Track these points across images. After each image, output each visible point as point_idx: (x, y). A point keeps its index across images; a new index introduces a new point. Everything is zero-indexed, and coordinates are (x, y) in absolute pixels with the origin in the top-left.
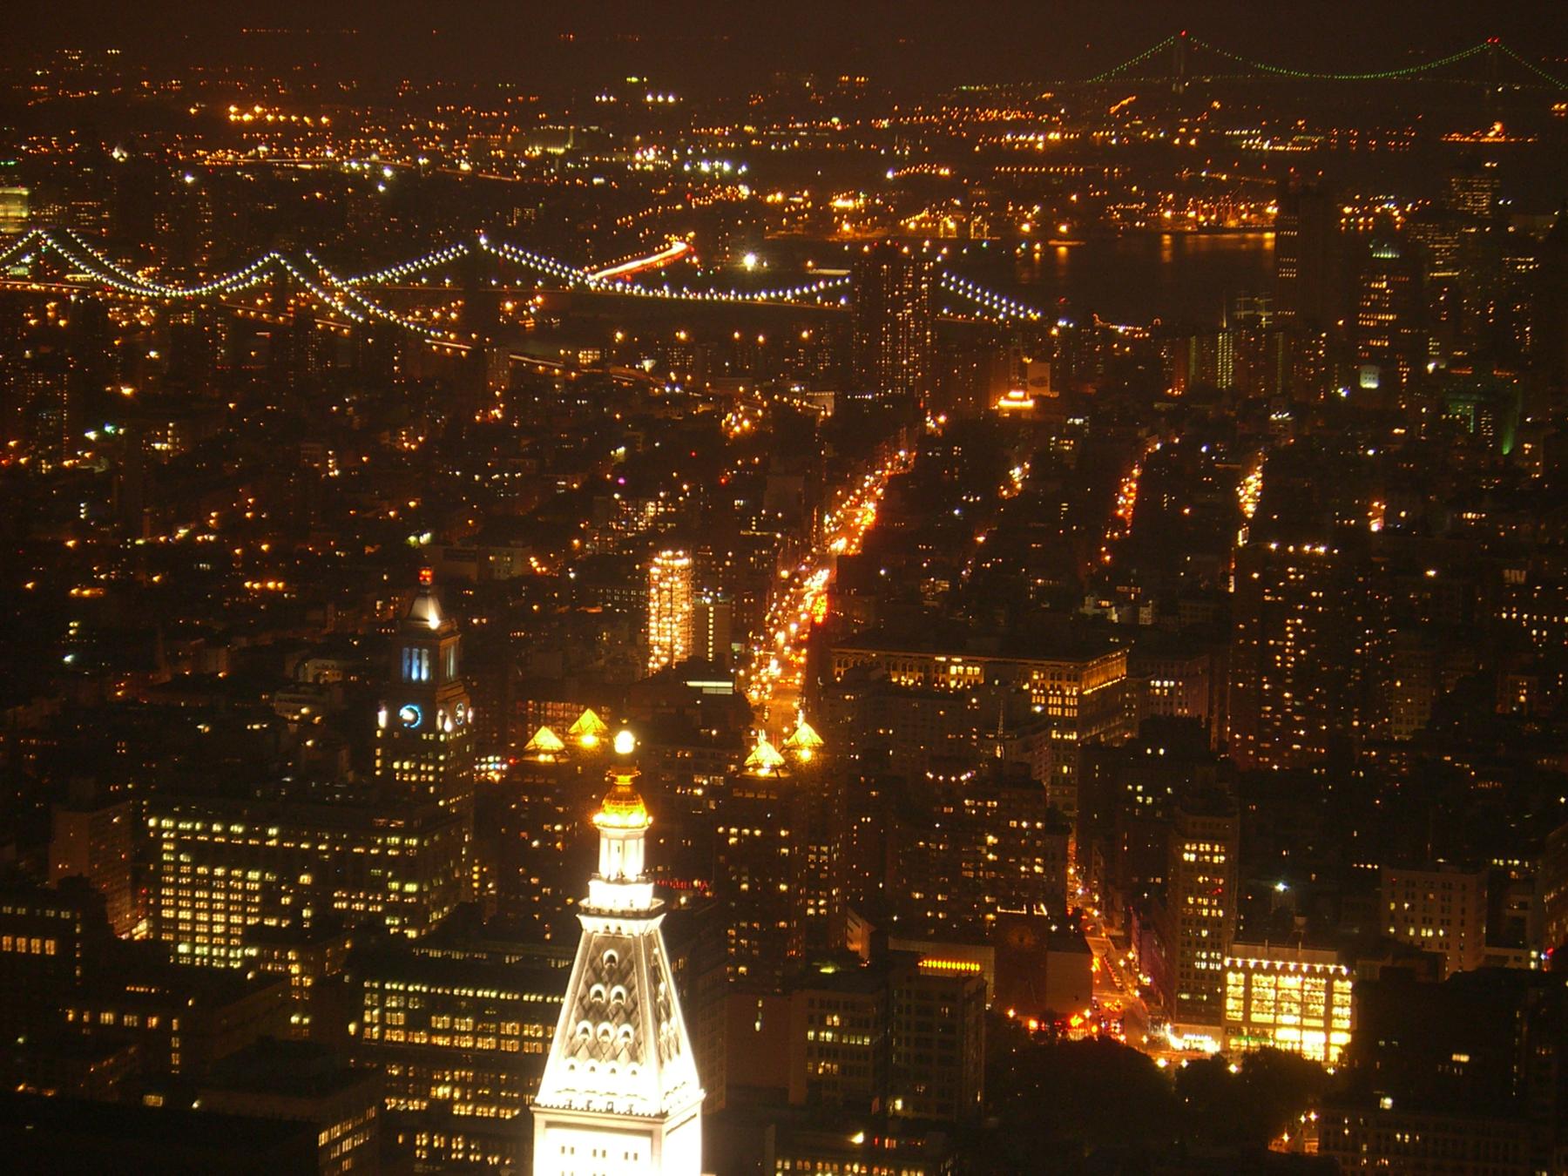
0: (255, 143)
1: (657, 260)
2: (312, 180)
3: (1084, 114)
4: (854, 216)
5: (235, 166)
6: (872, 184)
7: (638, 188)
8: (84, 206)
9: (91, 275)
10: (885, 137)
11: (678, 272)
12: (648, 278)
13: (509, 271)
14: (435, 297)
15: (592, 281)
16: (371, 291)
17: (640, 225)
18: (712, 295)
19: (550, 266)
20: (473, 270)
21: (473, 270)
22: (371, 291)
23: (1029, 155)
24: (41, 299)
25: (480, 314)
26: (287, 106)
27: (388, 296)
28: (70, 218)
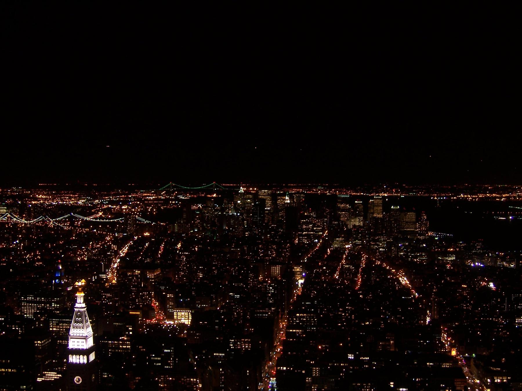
0: (40, 200)
1: (98, 216)
2: (48, 206)
3: (158, 193)
4: (126, 209)
5: (37, 204)
6: (129, 205)
7: (95, 206)
8: (48, 218)
9: (15, 219)
10: (130, 198)
11: (101, 217)
12: (96, 218)
13: (76, 218)
14: (65, 221)
15: (88, 219)
16: (56, 221)
17: (95, 211)
18: (105, 220)
19: (81, 217)
20: (71, 218)
21: (71, 218)
22: (56, 221)
23: (150, 200)
24: (8, 224)
25: (72, 224)
26: (45, 195)
27: (59, 222)
28: (13, 211)
